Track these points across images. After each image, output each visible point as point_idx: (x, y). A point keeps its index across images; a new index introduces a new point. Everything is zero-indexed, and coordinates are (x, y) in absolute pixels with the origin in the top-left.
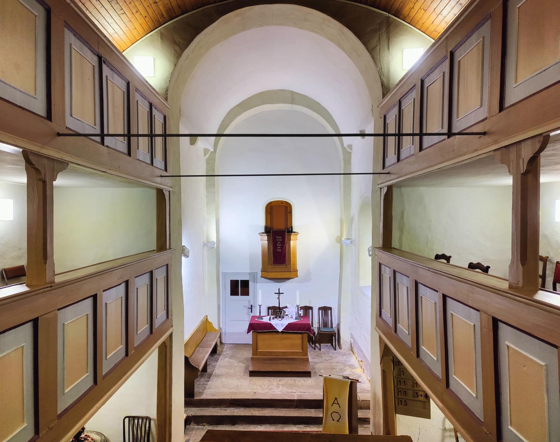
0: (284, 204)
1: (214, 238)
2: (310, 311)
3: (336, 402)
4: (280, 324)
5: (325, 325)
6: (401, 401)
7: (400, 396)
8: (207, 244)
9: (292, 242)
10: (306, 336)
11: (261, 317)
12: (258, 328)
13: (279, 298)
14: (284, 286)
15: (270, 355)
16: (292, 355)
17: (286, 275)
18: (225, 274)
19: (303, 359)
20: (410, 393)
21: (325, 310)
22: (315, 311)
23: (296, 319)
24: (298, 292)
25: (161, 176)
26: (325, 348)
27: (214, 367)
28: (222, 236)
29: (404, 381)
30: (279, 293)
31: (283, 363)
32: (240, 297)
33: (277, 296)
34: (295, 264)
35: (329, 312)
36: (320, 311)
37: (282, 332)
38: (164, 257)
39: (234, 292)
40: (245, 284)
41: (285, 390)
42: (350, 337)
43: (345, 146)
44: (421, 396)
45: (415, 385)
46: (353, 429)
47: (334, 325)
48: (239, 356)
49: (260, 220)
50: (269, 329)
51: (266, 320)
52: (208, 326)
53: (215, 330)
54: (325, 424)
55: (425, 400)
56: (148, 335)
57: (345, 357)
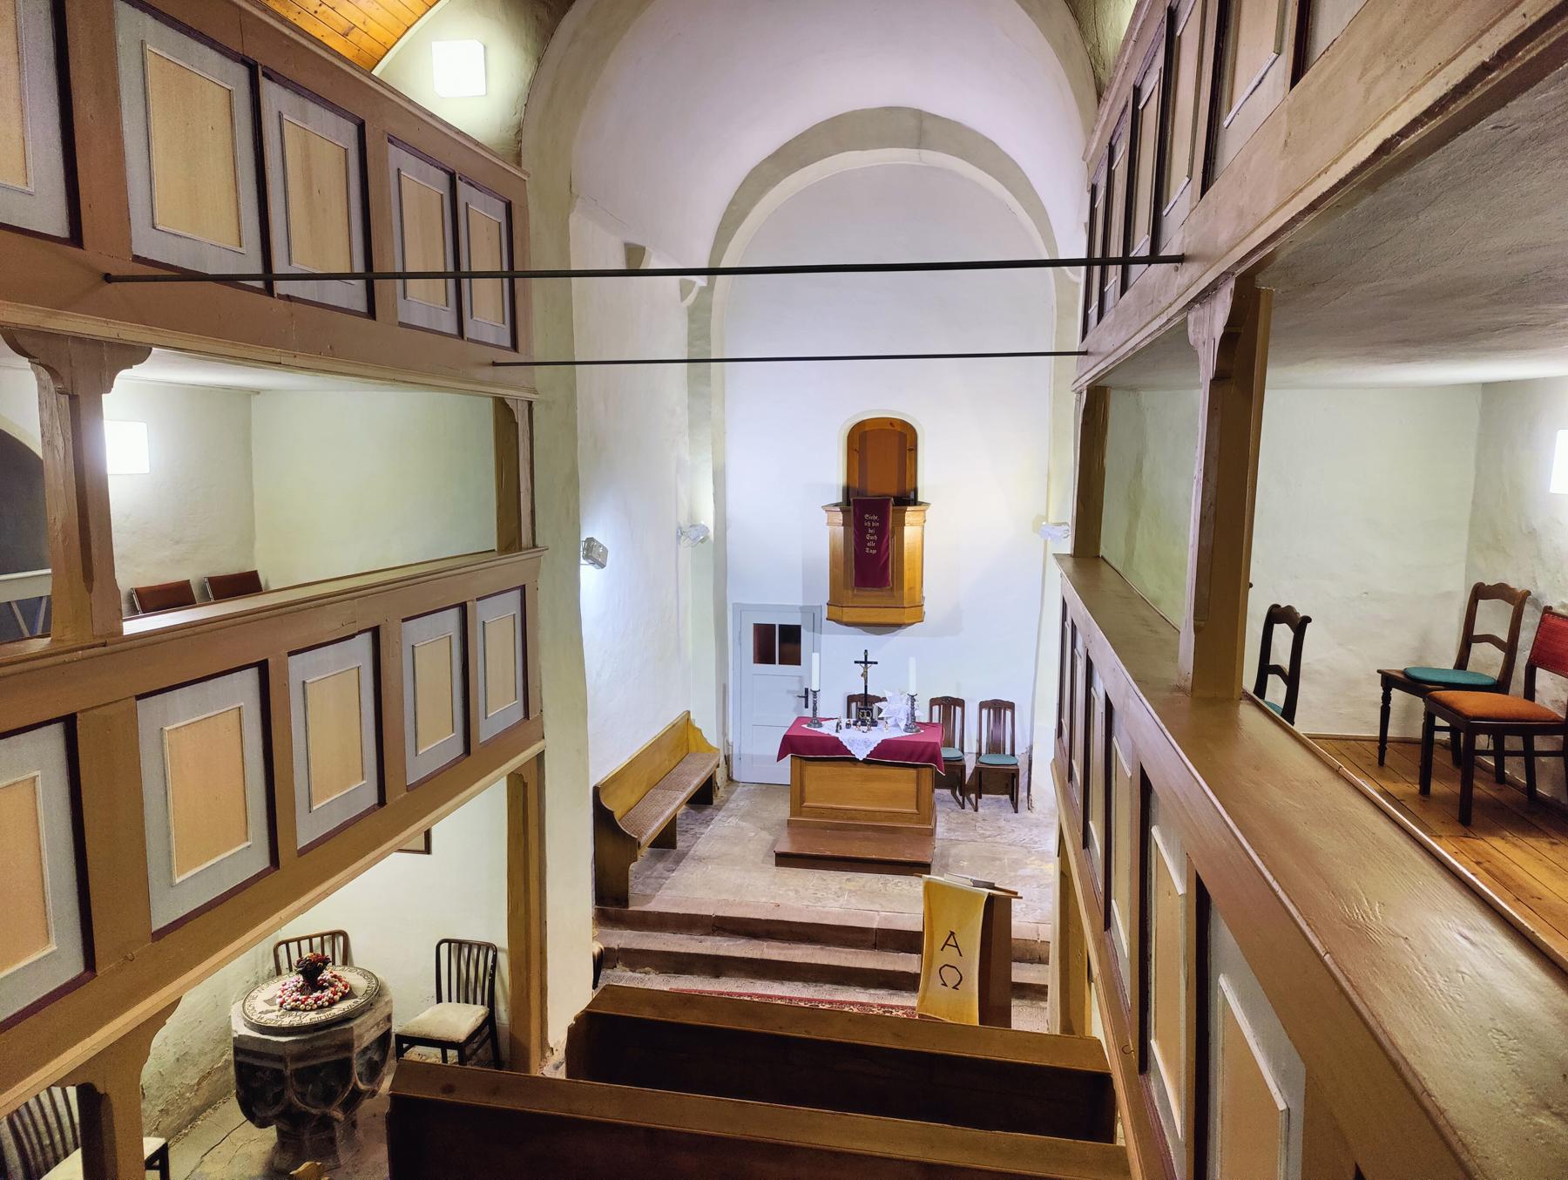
1: (707, 518)
2: (958, 709)
4: (861, 742)
5: (996, 747)
8: (688, 531)
9: (910, 533)
10: (927, 774)
11: (818, 722)
12: (806, 748)
13: (865, 675)
14: (882, 646)
16: (891, 820)
18: (740, 609)
19: (920, 832)
21: (998, 708)
22: (972, 710)
23: (907, 728)
24: (912, 660)
25: (494, 364)
26: (991, 804)
27: (696, 837)
28: (733, 509)
30: (866, 662)
31: (867, 839)
32: (777, 668)
33: (860, 668)
35: (1008, 713)
36: (985, 712)
37: (865, 761)
38: (513, 567)
39: (764, 655)
40: (791, 635)
41: (855, 903)
46: (994, 1010)
47: (1020, 750)
48: (765, 815)
49: (830, 473)
50: (832, 752)
51: (827, 729)
52: (691, 737)
53: (710, 748)
54: (925, 991)
56: (504, 750)
57: (1035, 831)
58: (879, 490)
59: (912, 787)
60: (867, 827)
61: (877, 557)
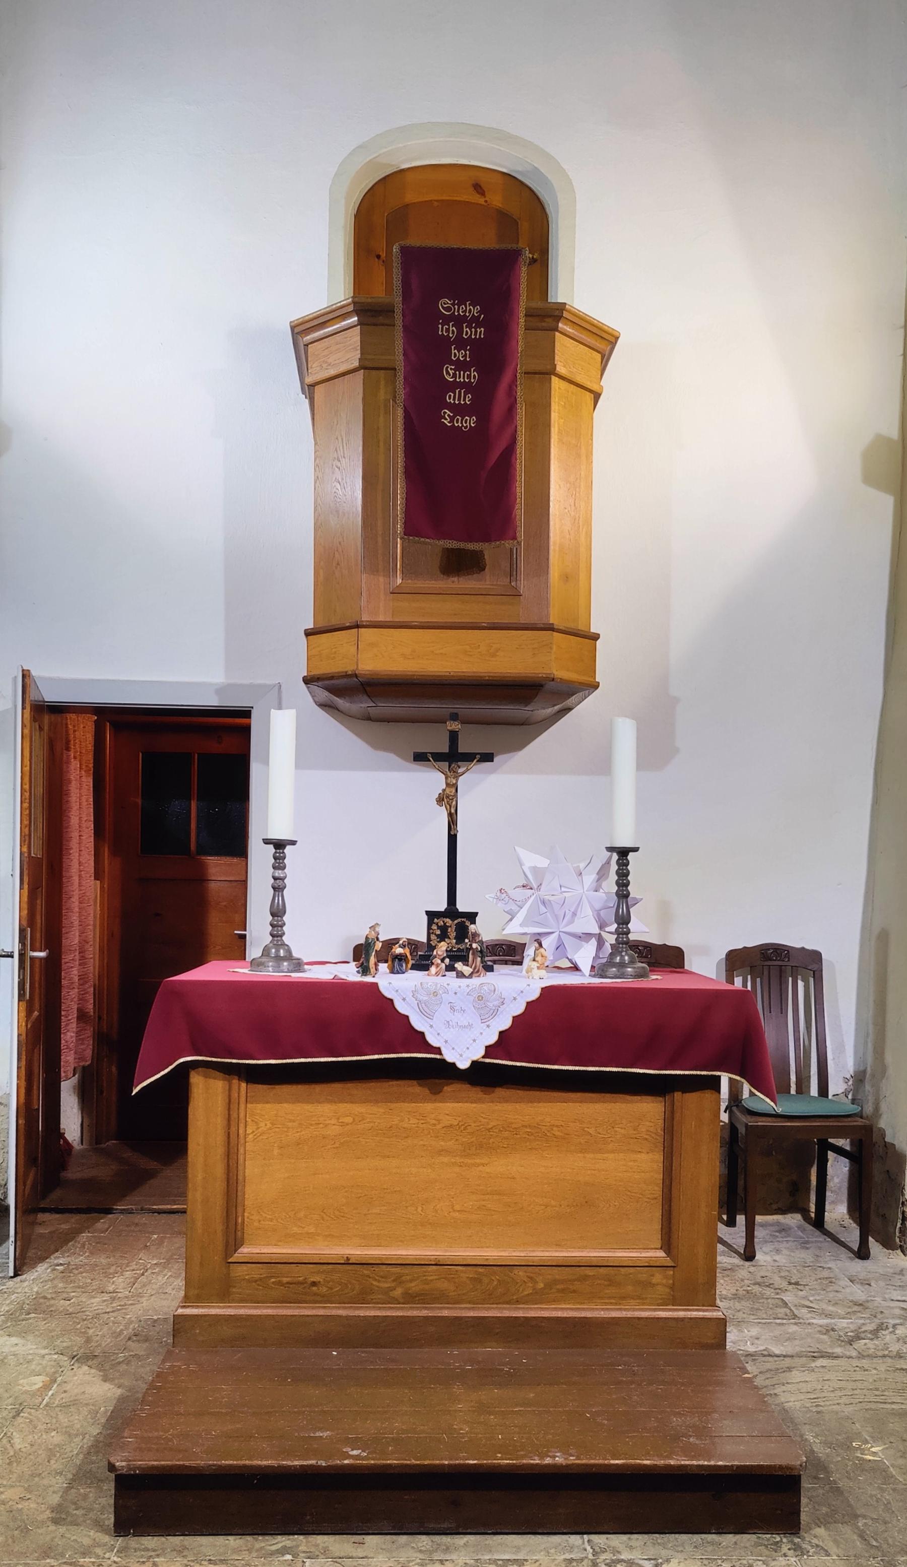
13: (448, 799)
15: (363, 1298)
16: (566, 1292)
31: (487, 1375)
33: (433, 780)
34: (578, 576)
37: (482, 1076)
58: (453, 327)
59: (647, 1164)
60: (483, 1329)
61: (482, 432)
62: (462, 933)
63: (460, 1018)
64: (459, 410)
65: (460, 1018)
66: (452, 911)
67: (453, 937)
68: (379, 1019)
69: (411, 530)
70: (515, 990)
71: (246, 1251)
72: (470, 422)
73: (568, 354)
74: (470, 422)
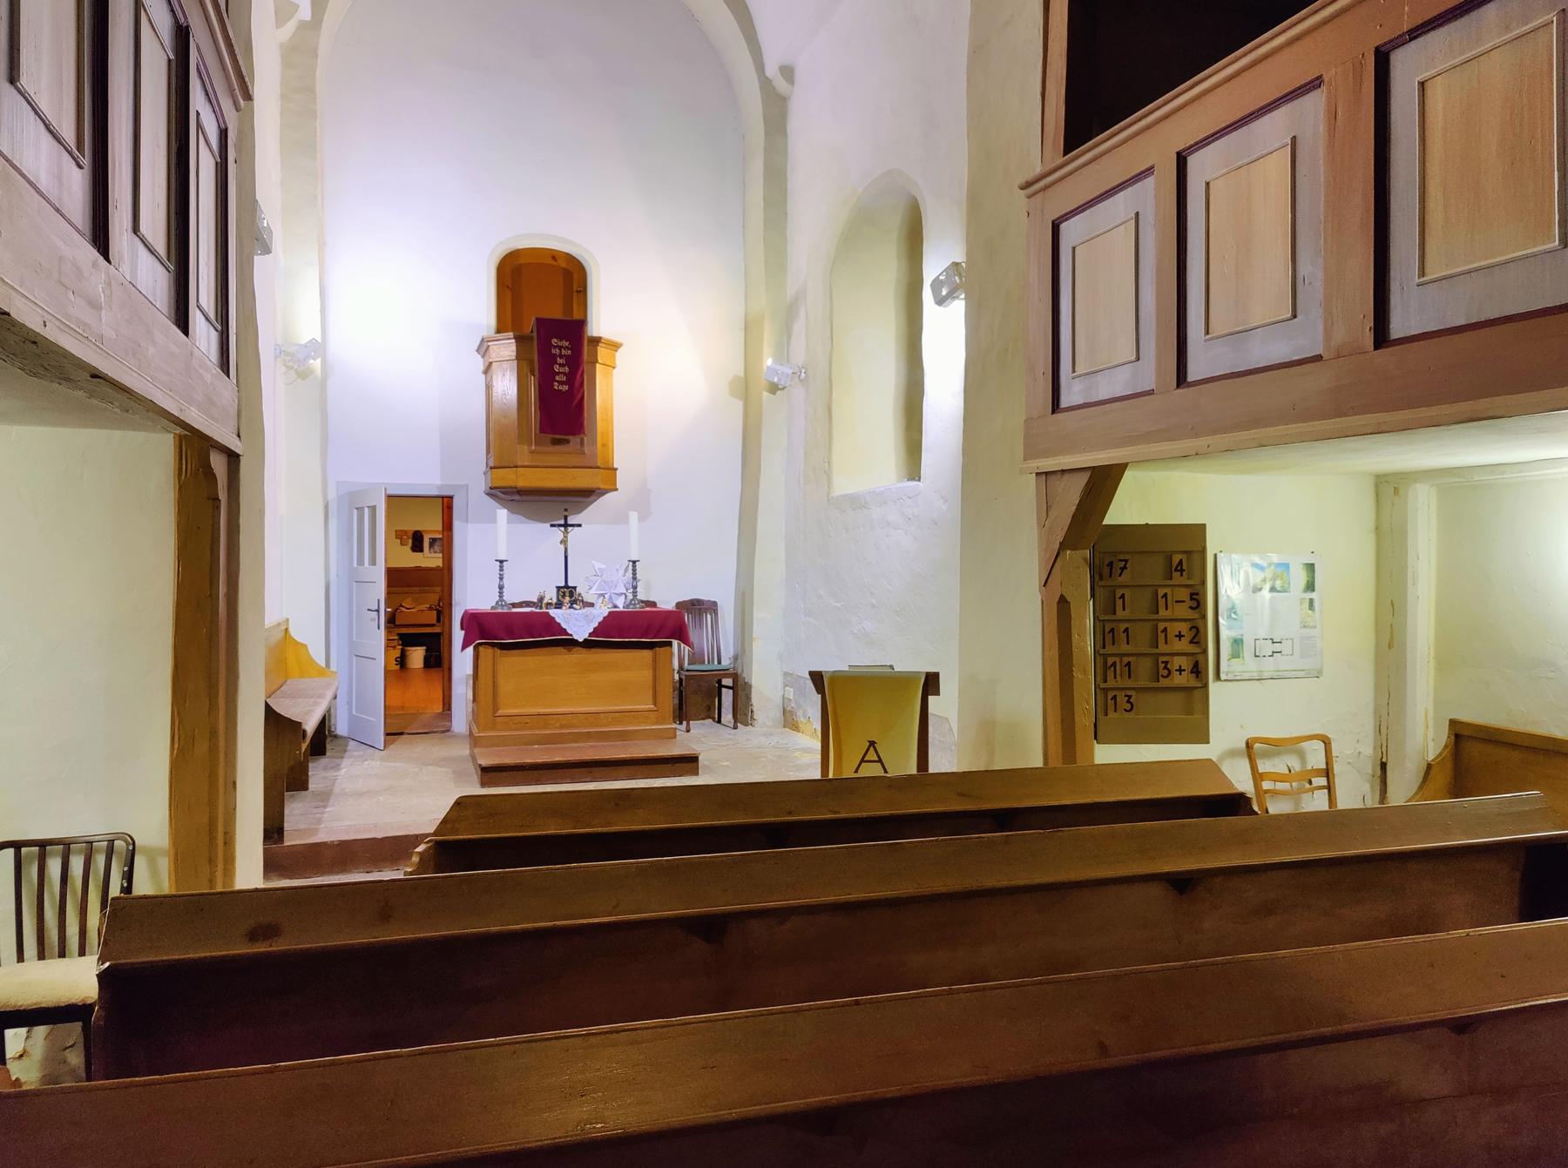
0: (563, 264)
3: (872, 756)
6: (1114, 698)
7: (1111, 683)
13: (564, 542)
17: (580, 479)
20: (1144, 667)
29: (1126, 630)
33: (558, 533)
34: (608, 446)
37: (588, 644)
42: (780, 686)
43: (771, 71)
44: (1180, 670)
45: (1161, 636)
47: (726, 663)
55: (1191, 681)
59: (647, 675)
62: (571, 595)
63: (579, 624)
64: (560, 383)
65: (579, 624)
66: (566, 586)
67: (568, 594)
68: (552, 626)
69: (542, 430)
70: (601, 612)
71: (500, 712)
72: (565, 388)
73: (602, 351)
74: (565, 388)
